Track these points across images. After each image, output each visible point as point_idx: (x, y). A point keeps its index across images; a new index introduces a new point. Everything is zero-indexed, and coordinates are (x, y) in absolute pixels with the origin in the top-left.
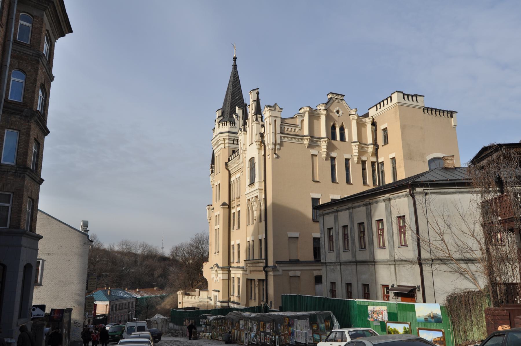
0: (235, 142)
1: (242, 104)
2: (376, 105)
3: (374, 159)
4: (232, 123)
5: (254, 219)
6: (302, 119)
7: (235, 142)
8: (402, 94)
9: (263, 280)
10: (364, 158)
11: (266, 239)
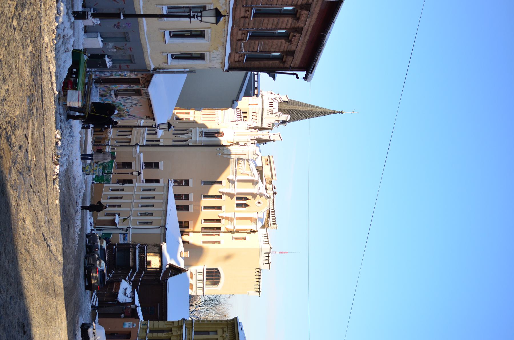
0: (254, 114)
1: (293, 119)
2: (267, 234)
3: (223, 229)
4: (272, 111)
5: (176, 135)
6: (249, 174)
7: (254, 114)
8: (269, 252)
9: (130, 142)
10: (223, 221)
11: (158, 146)
